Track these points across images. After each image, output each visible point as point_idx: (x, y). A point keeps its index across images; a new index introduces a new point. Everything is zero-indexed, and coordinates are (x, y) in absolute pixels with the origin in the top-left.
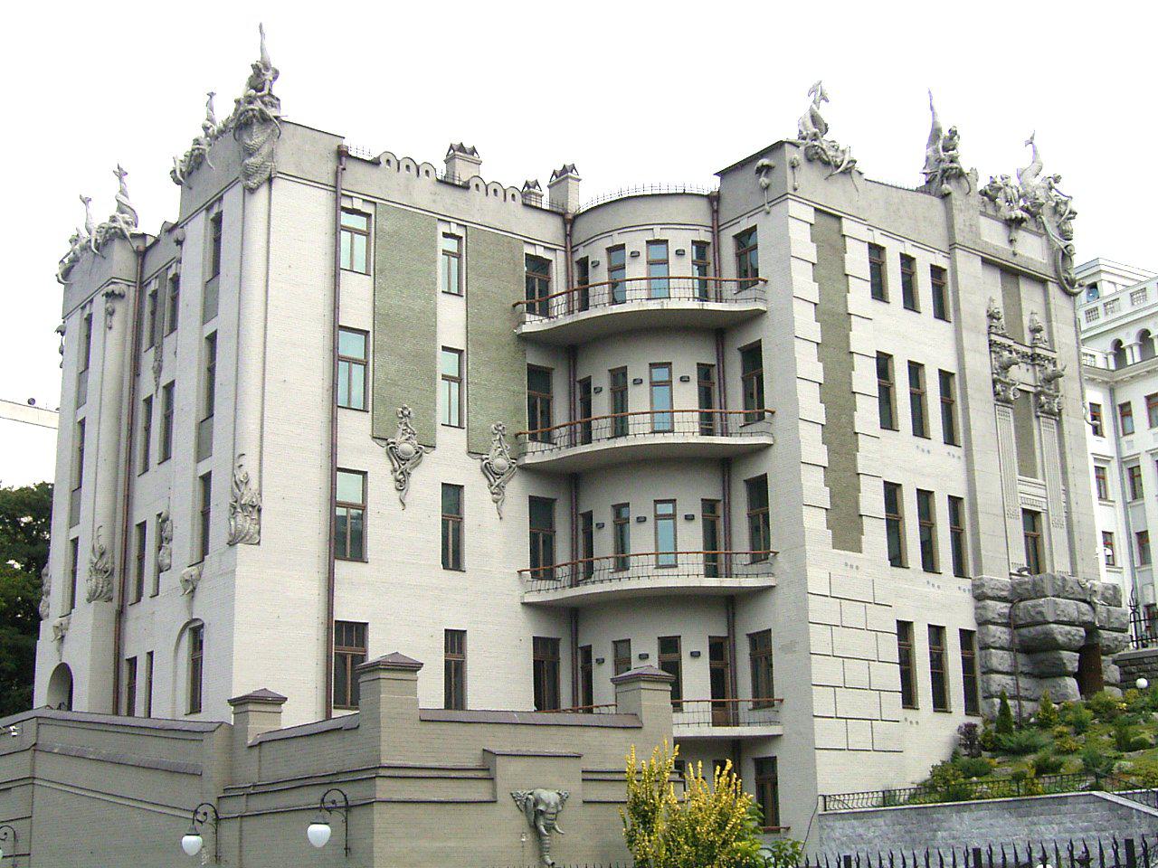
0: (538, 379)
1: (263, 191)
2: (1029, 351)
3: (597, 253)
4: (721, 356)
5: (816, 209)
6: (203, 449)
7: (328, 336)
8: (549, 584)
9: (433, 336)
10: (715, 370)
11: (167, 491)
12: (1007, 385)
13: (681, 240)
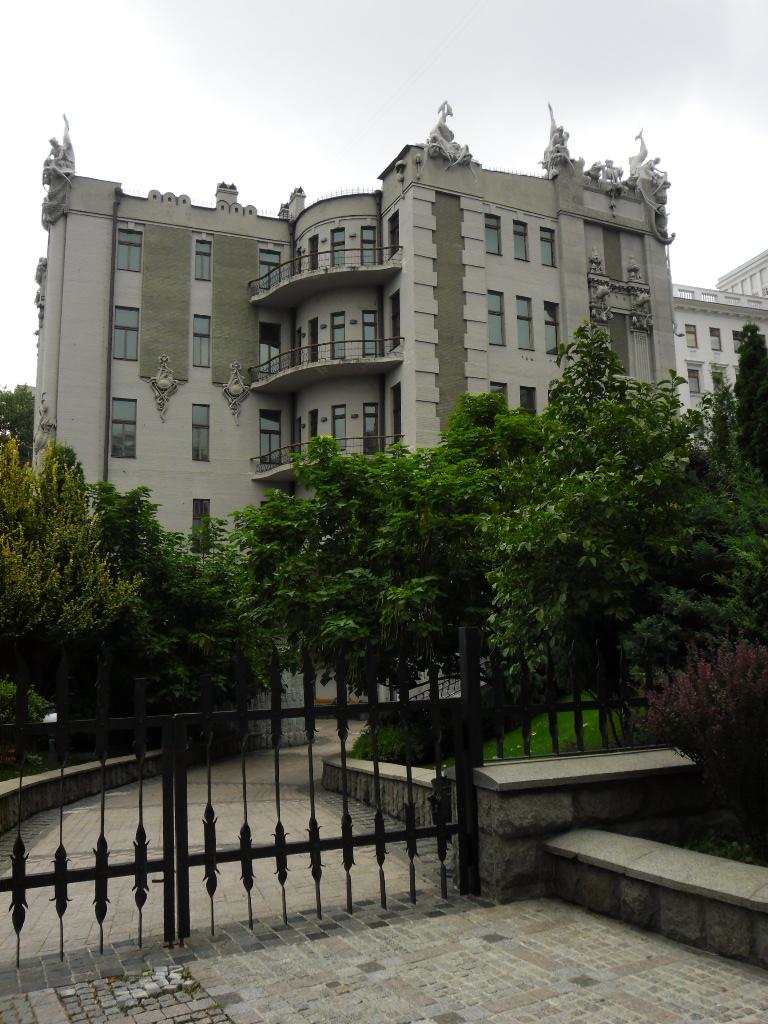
2: (625, 286)
3: (304, 245)
5: (437, 192)
9: (185, 305)
13: (352, 227)
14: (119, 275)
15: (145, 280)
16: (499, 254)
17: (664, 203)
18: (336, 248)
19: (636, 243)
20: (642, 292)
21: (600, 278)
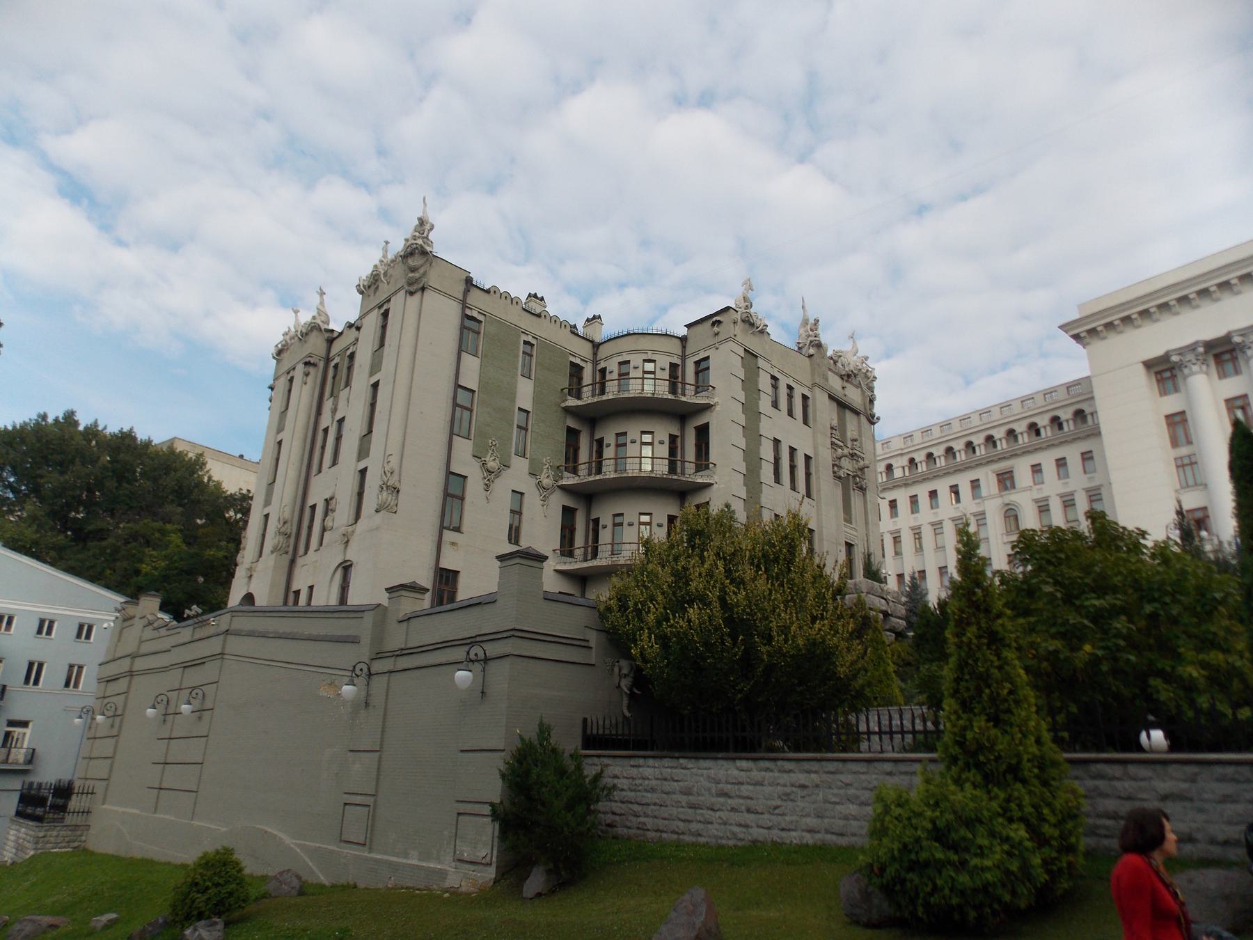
0: (572, 434)
1: (418, 295)
3: (613, 366)
4: (683, 429)
6: (363, 452)
8: (569, 559)
9: (512, 398)
10: (679, 440)
11: (334, 483)
12: (840, 467)
13: (664, 362)
14: (465, 356)
19: (855, 417)
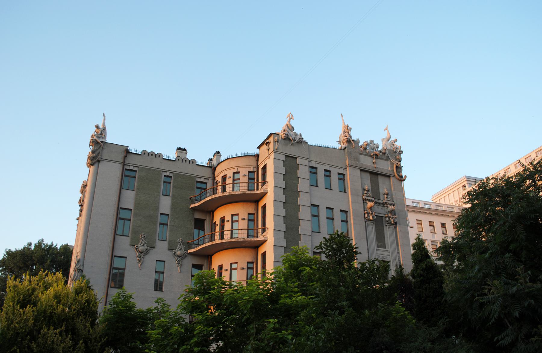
2: (382, 202)
3: (219, 179)
7: (116, 211)
9: (157, 209)
13: (244, 171)
15: (137, 195)
16: (317, 186)
17: (400, 161)
18: (235, 182)
20: (391, 205)
21: (369, 198)
